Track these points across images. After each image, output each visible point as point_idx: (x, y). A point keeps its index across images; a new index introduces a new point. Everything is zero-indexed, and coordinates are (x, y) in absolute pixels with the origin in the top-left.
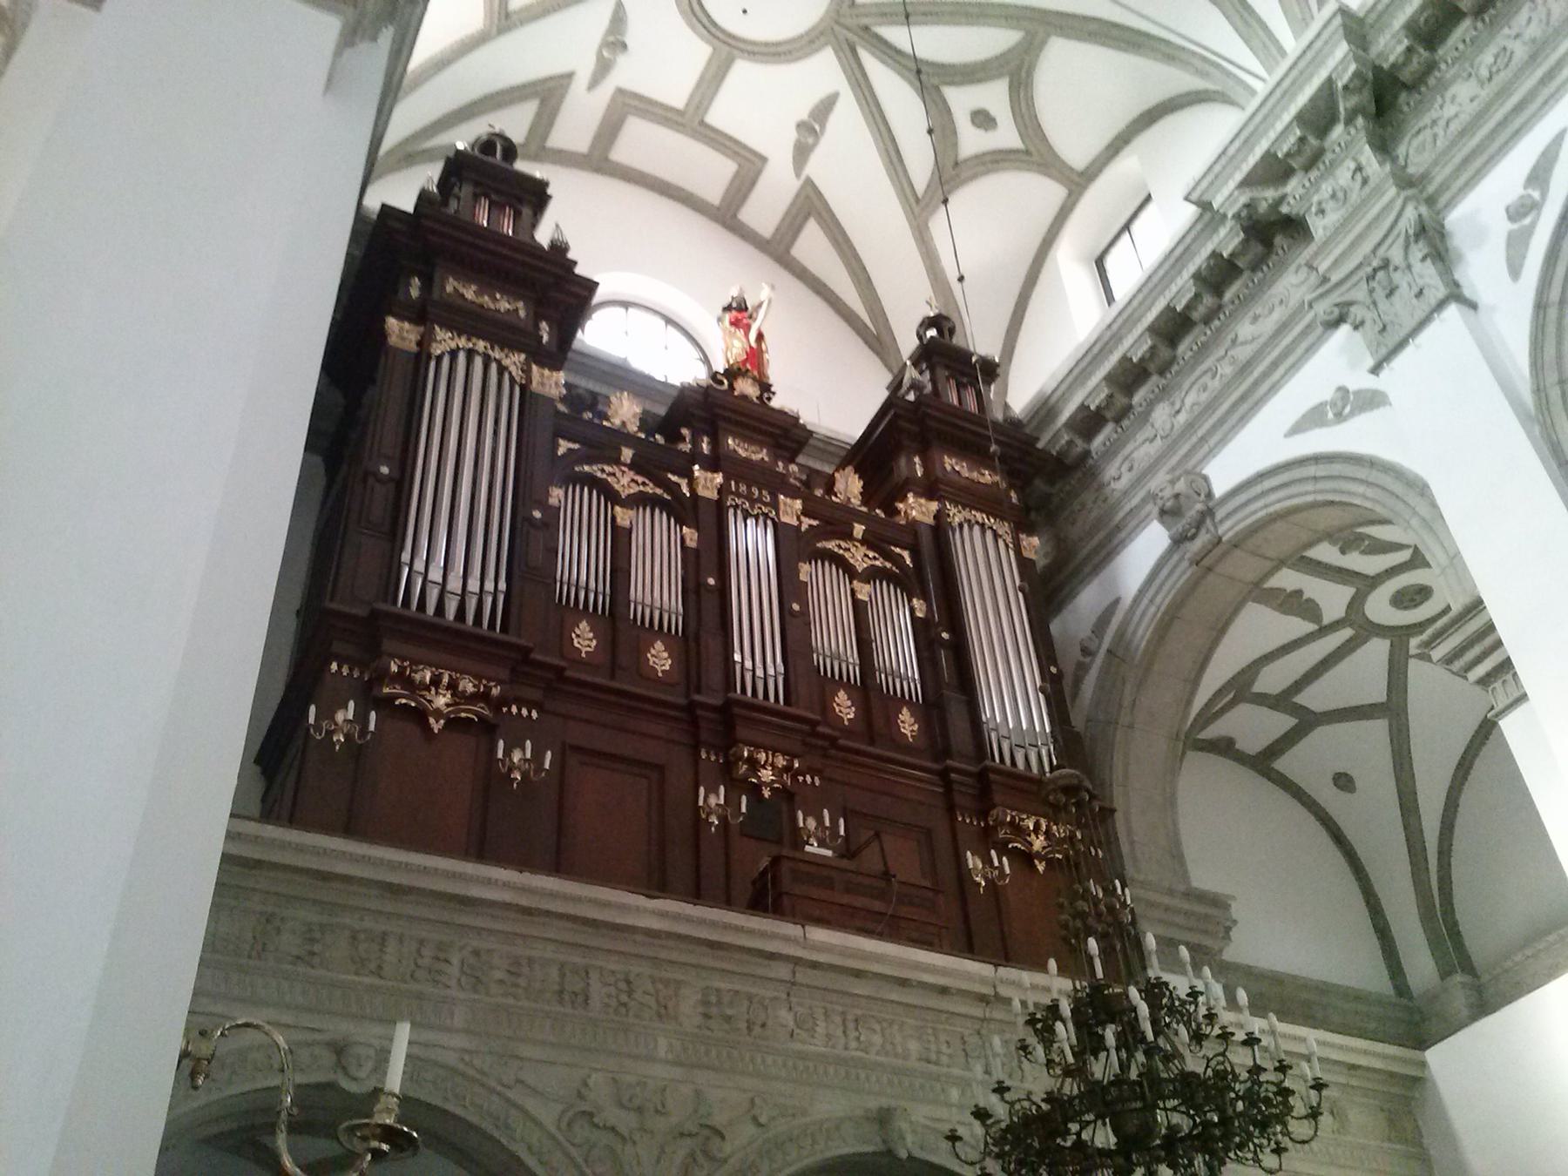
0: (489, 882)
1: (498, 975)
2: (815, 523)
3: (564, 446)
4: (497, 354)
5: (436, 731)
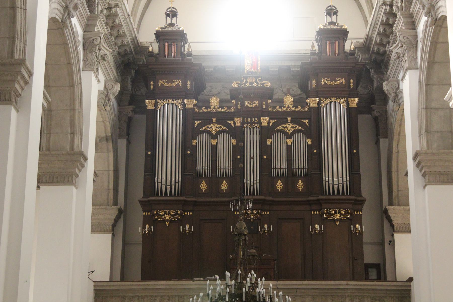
0: (160, 285)
2: (274, 121)
3: (197, 123)
4: (175, 101)
5: (168, 225)
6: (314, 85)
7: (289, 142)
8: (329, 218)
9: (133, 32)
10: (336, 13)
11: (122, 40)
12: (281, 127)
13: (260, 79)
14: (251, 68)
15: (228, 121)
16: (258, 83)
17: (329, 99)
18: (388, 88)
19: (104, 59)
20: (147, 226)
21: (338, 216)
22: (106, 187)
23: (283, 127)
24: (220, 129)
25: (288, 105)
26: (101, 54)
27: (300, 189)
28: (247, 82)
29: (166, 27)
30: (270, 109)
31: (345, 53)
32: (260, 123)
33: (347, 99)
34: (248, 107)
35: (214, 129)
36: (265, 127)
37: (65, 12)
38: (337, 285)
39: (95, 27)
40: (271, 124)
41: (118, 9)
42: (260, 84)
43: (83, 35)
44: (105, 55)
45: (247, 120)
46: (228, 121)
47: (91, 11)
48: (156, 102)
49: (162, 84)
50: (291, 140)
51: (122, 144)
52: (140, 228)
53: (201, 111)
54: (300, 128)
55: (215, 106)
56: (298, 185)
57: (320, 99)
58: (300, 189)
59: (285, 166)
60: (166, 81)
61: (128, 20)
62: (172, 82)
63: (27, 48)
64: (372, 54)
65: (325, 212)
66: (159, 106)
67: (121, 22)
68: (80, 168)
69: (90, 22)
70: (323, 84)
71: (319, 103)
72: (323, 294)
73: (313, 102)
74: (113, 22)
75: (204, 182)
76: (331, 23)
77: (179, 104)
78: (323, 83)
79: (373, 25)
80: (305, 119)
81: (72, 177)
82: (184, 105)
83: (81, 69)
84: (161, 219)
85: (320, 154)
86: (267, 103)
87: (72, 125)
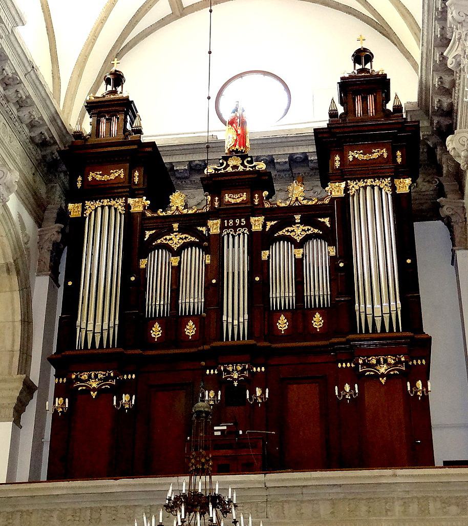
0: (57, 488)
1: (70, 517)
2: (273, 223)
4: (113, 202)
6: (337, 164)
8: (368, 373)
11: (29, 112)
12: (284, 231)
13: (249, 159)
14: (235, 145)
15: (199, 228)
16: (246, 167)
17: (363, 182)
18: (454, 145)
21: (383, 369)
22: (9, 347)
23: (288, 231)
24: (185, 241)
25: (297, 198)
28: (228, 165)
30: (267, 206)
32: (248, 225)
33: (392, 181)
34: (229, 203)
35: (176, 240)
38: (375, 477)
42: (249, 167)
45: (228, 223)
46: (199, 228)
48: (83, 206)
49: (93, 178)
50: (301, 250)
53: (155, 215)
54: (316, 231)
55: (177, 207)
56: (315, 321)
57: (347, 183)
59: (292, 293)
60: (100, 173)
61: (34, 77)
62: (109, 174)
65: (361, 362)
67: (16, 73)
70: (351, 160)
71: (346, 189)
72: (350, 497)
73: (336, 189)
76: (363, 70)
77: (120, 205)
78: (351, 158)
79: (424, 56)
80: (324, 217)
82: (128, 207)
86: (261, 197)
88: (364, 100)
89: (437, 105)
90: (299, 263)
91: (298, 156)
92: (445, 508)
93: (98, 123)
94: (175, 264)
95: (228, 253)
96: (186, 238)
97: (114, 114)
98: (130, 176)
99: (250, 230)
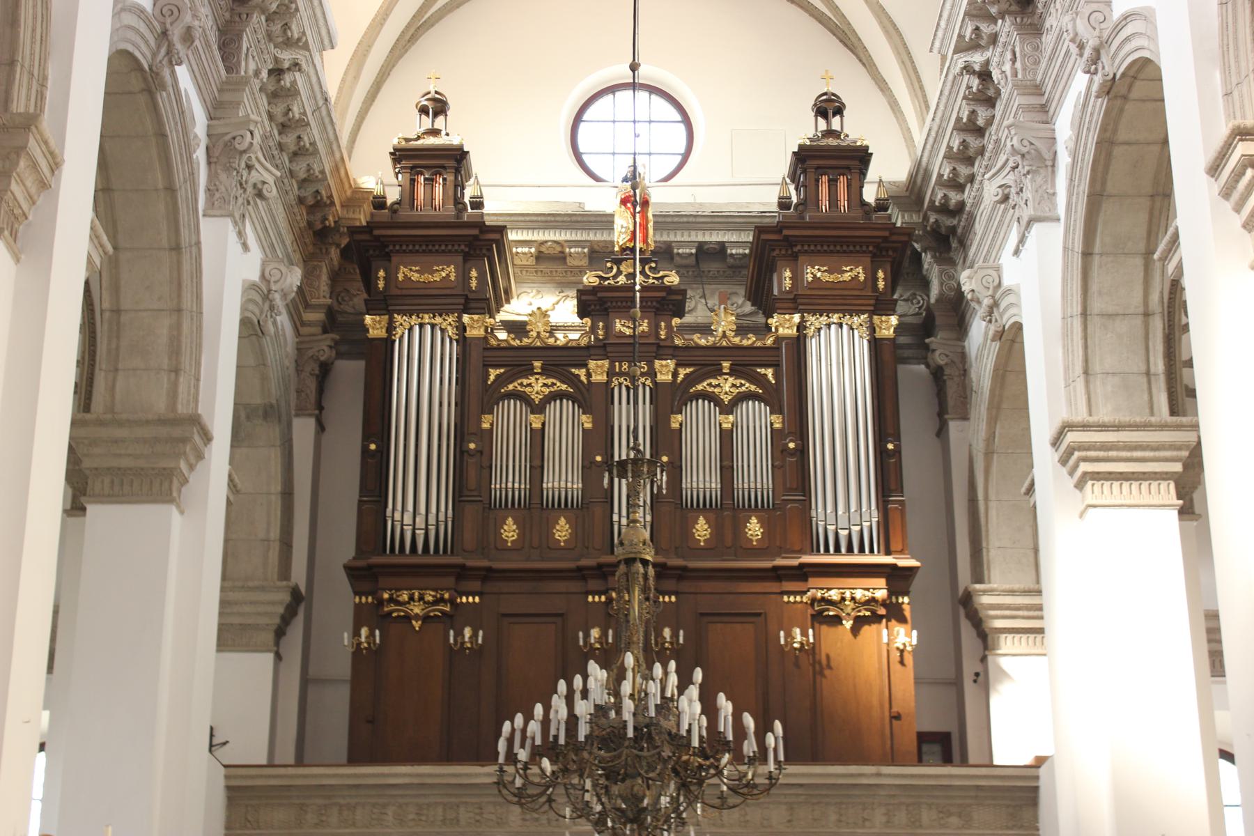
0: (396, 775)
1: (411, 816)
2: (688, 370)
3: (493, 373)
4: (438, 320)
5: (417, 629)
6: (788, 283)
7: (727, 421)
9: (335, 147)
10: (839, 111)
11: (308, 165)
12: (705, 384)
13: (653, 265)
15: (573, 370)
16: (647, 277)
17: (826, 318)
18: (973, 287)
19: (260, 195)
20: (364, 632)
23: (710, 385)
24: (552, 390)
25: (724, 332)
26: (252, 181)
27: (755, 538)
28: (619, 273)
29: (419, 138)
30: (678, 342)
31: (864, 204)
32: (652, 374)
33: (871, 318)
36: (664, 384)
37: (159, 47)
38: (852, 775)
39: (238, 108)
40: (681, 377)
41: (297, 74)
42: (654, 278)
43: (209, 126)
44: (264, 183)
45: (621, 366)
46: (573, 370)
47: (229, 70)
50: (731, 418)
51: (304, 428)
52: (346, 635)
54: (753, 388)
55: (538, 333)
56: (750, 530)
57: (803, 317)
58: (755, 538)
59: (715, 484)
60: (417, 268)
61: (324, 113)
62: (432, 272)
63: (48, 95)
64: (929, 213)
66: (399, 331)
67: (305, 114)
68: (192, 459)
69: (227, 97)
70: (810, 279)
71: (801, 327)
72: (815, 801)
74: (287, 114)
75: (510, 521)
76: (830, 133)
77: (450, 324)
79: (933, 134)
81: (171, 482)
82: (462, 328)
83: (201, 213)
84: (402, 614)
85: (802, 451)
87: (175, 349)
88: (833, 183)
89: (941, 200)
90: (726, 438)
91: (711, 246)
92: (942, 818)
93: (413, 181)
94: (537, 425)
95: (621, 415)
96: (553, 384)
97: (439, 170)
98: (465, 278)
99: (655, 383)
